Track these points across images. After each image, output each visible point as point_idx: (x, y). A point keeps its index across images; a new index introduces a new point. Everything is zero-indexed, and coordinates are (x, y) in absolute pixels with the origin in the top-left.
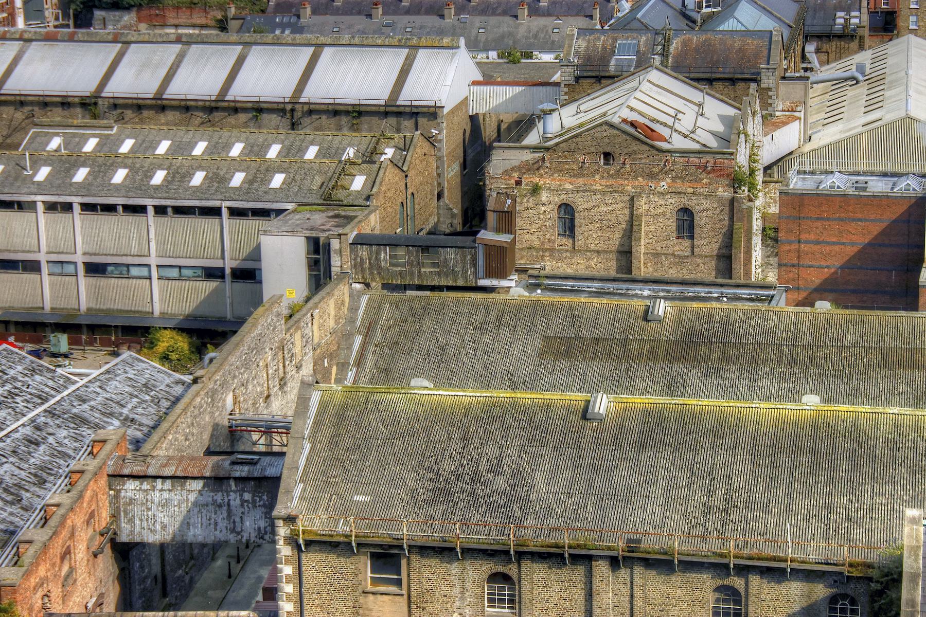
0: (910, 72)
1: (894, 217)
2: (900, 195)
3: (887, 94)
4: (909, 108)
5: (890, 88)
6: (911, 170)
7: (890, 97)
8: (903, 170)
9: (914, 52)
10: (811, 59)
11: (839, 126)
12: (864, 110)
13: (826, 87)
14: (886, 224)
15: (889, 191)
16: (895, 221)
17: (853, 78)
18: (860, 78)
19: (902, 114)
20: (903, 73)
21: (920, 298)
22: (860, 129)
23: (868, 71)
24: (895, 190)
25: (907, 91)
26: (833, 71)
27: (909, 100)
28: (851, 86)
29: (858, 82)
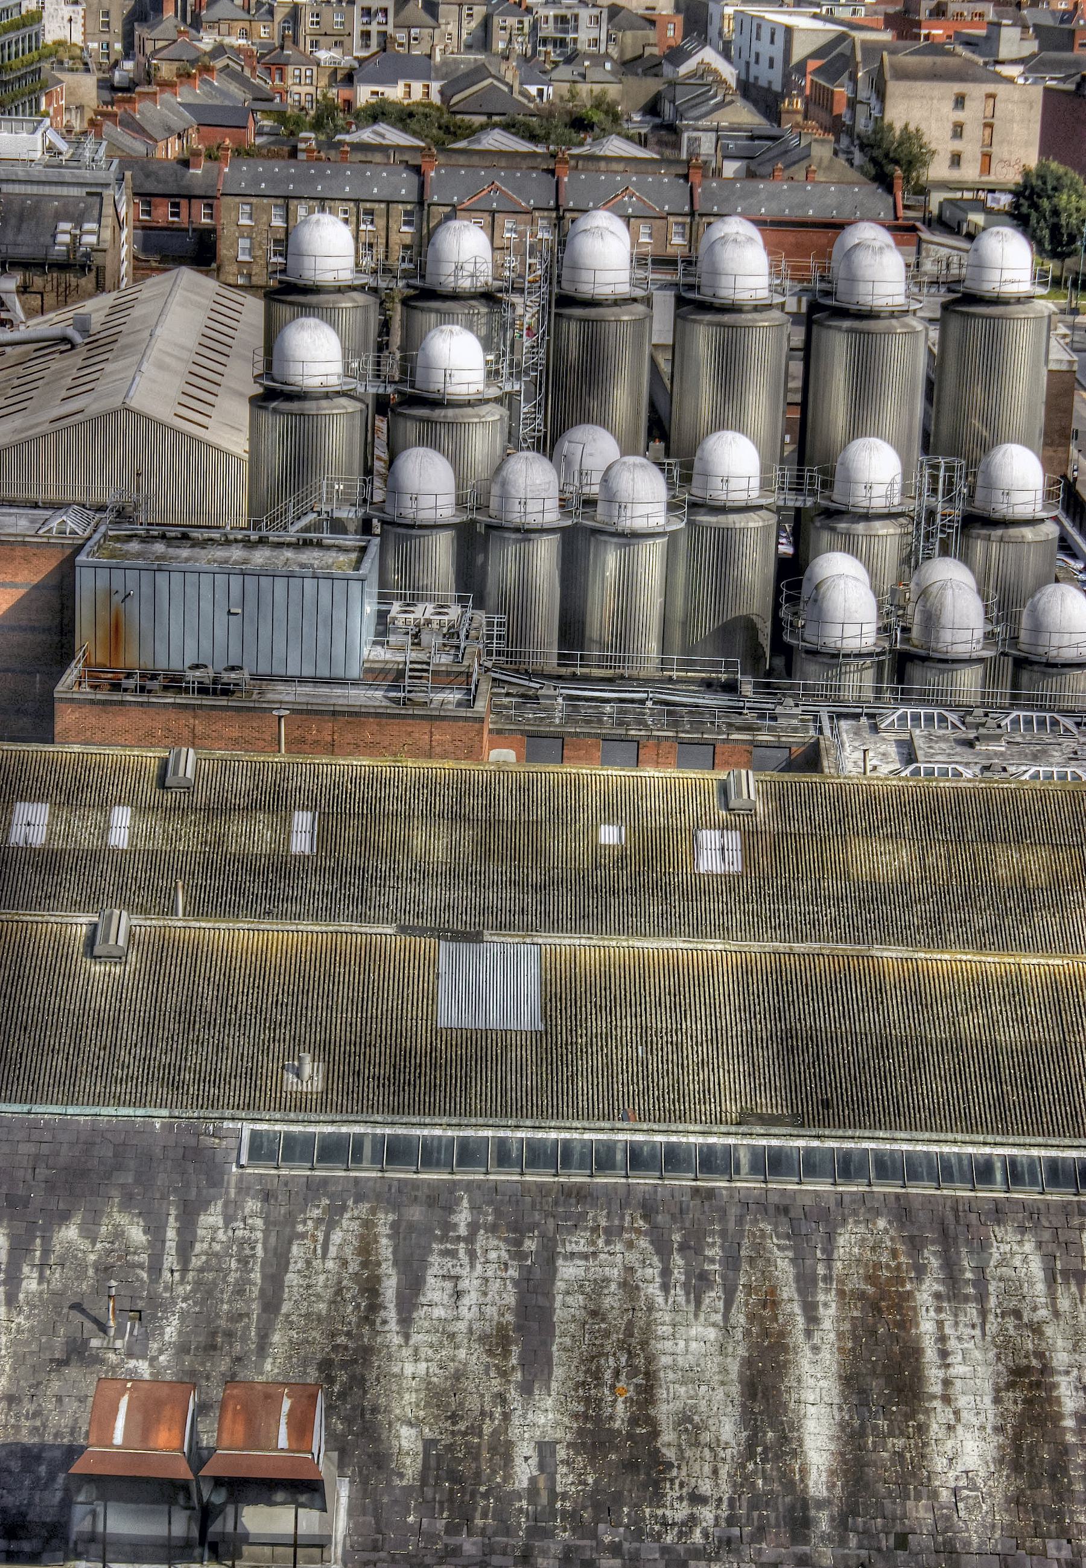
0: (158, 331)
1: (36, 579)
2: (44, 540)
3: (109, 367)
4: (131, 393)
5: (116, 359)
6: (78, 498)
7: (111, 373)
8: (69, 498)
9: (179, 295)
10: (9, 304)
11: (17, 421)
12: (64, 394)
13: (27, 353)
14: (22, 591)
15: (33, 533)
16: (36, 587)
17: (65, 340)
18: (78, 338)
19: (116, 402)
20: (147, 333)
21: (56, 720)
22: (46, 428)
23: (95, 327)
24: (41, 532)
25: (141, 363)
26: (46, 326)
27: (137, 379)
28: (62, 352)
29: (73, 347)
